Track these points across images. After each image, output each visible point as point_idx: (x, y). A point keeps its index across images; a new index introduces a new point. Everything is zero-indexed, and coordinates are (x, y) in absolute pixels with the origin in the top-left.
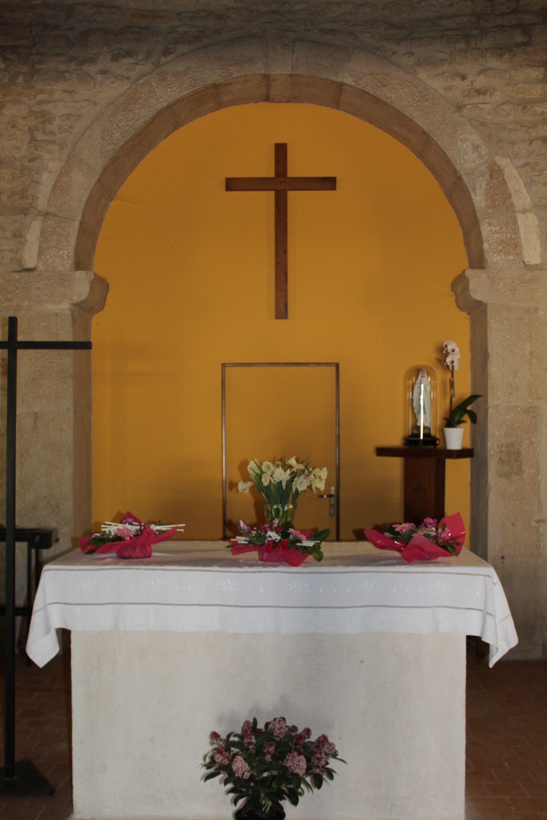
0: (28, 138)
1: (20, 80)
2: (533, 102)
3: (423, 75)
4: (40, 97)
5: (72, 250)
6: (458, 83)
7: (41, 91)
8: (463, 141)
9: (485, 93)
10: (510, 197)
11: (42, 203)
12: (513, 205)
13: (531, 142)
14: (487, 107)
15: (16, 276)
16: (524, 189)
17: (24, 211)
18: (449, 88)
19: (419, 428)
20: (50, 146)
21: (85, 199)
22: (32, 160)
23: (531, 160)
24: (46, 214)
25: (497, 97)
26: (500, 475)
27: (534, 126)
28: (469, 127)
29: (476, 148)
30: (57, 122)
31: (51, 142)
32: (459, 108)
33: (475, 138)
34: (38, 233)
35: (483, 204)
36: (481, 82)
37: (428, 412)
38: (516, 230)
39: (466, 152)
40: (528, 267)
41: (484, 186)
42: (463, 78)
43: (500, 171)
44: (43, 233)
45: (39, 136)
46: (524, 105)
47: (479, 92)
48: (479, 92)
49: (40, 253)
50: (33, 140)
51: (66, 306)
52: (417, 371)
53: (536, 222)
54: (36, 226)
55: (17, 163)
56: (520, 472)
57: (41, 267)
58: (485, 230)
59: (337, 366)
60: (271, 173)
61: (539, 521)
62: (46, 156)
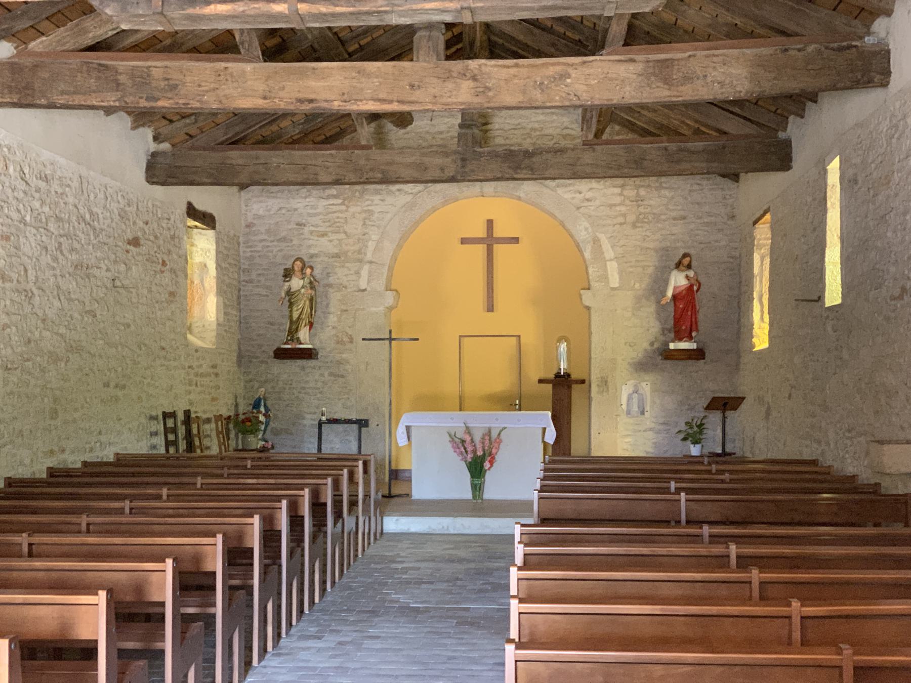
0: (362, 223)
1: (357, 194)
2: (615, 205)
3: (560, 191)
4: (367, 203)
5: (384, 281)
6: (578, 195)
7: (368, 200)
8: (580, 225)
9: (591, 201)
10: (603, 253)
11: (369, 256)
12: (605, 258)
13: (614, 225)
14: (592, 208)
15: (357, 294)
16: (611, 249)
17: (360, 261)
18: (573, 198)
19: (560, 369)
20: (372, 228)
21: (391, 255)
22: (364, 235)
23: (614, 234)
24: (371, 262)
25: (597, 203)
26: (598, 392)
27: (616, 217)
28: (583, 219)
29: (586, 229)
30: (376, 215)
31: (373, 225)
32: (578, 208)
33: (587, 225)
34: (367, 272)
35: (590, 257)
36: (589, 195)
37: (565, 361)
38: (606, 270)
39: (581, 231)
40: (613, 289)
41: (590, 247)
42: (580, 193)
43: (599, 240)
44: (370, 272)
45: (367, 222)
46: (611, 206)
47: (588, 200)
48: (588, 200)
49: (369, 282)
50: (364, 224)
51: (382, 308)
52: (559, 340)
53: (617, 266)
54: (366, 267)
55: (356, 237)
56: (608, 391)
57: (369, 289)
58: (591, 270)
59: (519, 336)
60: (485, 236)
61: (617, 415)
62: (371, 232)
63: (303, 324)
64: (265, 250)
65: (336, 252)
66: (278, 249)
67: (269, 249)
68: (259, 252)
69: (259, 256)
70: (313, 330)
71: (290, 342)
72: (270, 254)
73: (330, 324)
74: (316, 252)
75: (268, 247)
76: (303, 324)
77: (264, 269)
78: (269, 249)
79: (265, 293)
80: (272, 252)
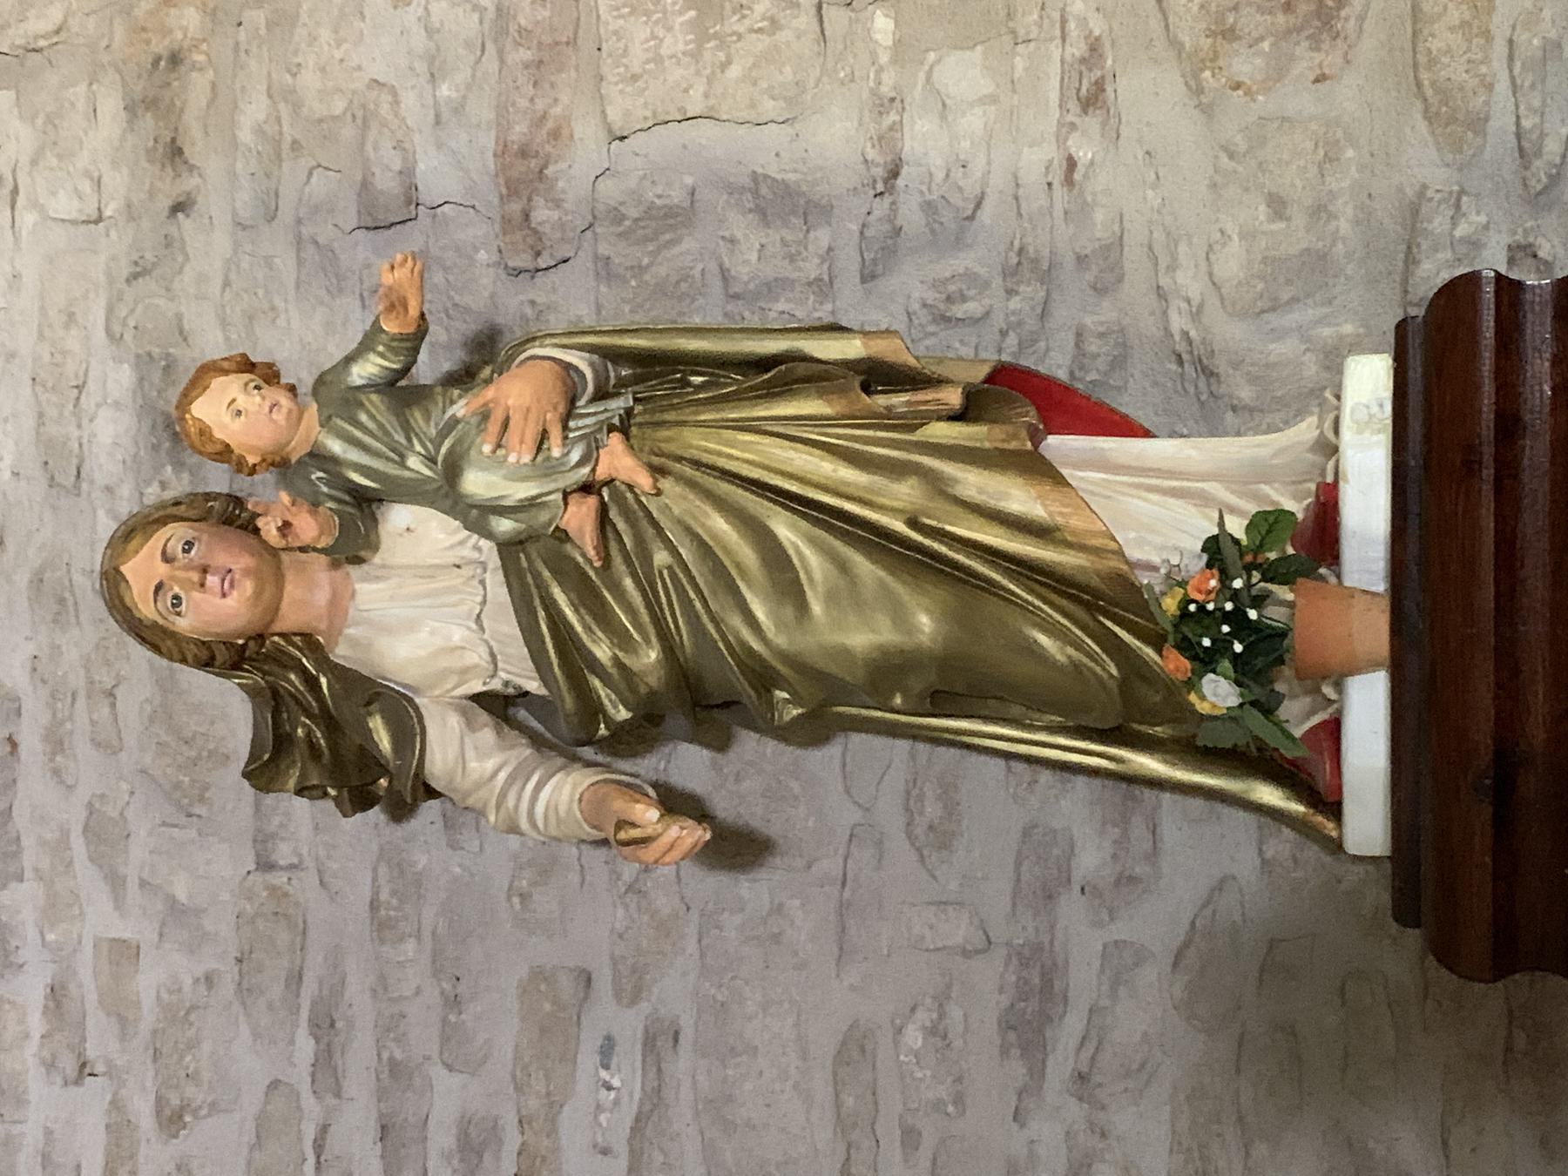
63: (1020, 497)
64: (100, 1042)
65: (111, 105)
66: (87, 876)
67: (87, 981)
68: (119, 1130)
69: (172, 1120)
70: (1128, 405)
71: (1299, 718)
72: (148, 982)
73: (1037, 159)
74: (122, 378)
75: (56, 994)
76: (1020, 497)
77: (326, 1068)
78: (87, 981)
79: (626, 1077)
80: (124, 953)
